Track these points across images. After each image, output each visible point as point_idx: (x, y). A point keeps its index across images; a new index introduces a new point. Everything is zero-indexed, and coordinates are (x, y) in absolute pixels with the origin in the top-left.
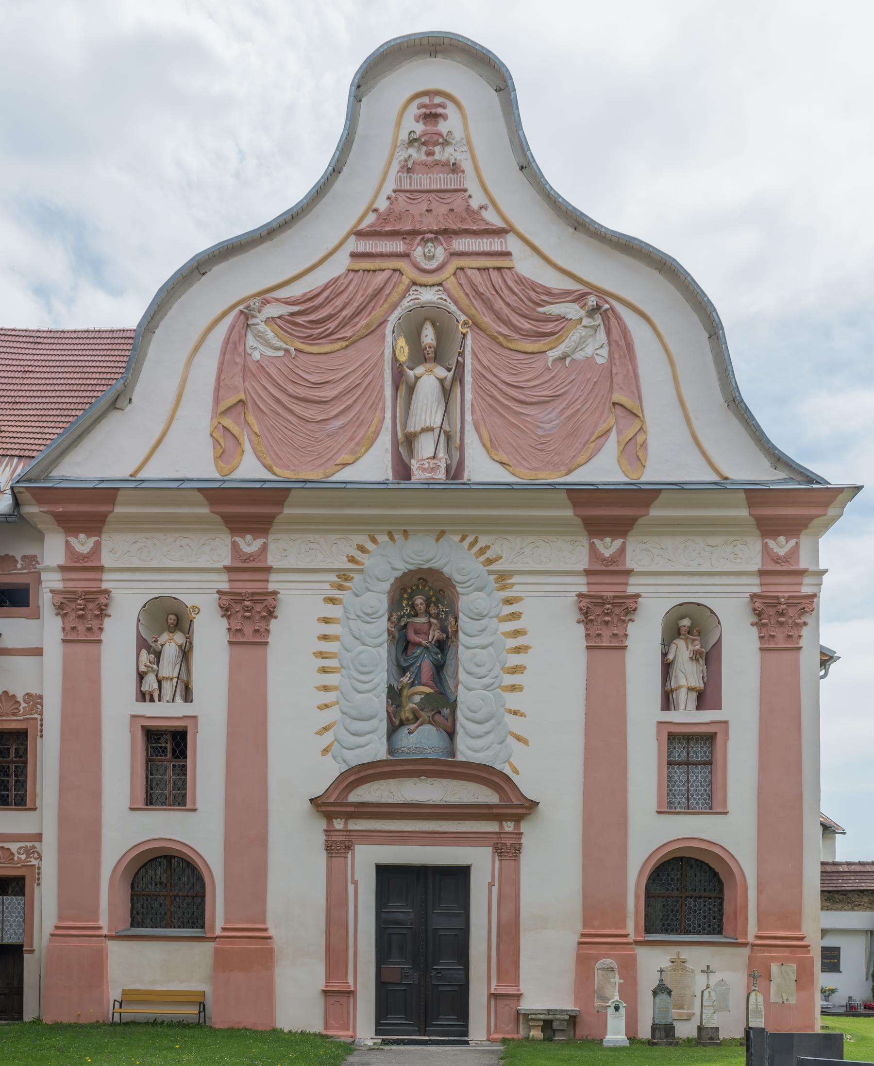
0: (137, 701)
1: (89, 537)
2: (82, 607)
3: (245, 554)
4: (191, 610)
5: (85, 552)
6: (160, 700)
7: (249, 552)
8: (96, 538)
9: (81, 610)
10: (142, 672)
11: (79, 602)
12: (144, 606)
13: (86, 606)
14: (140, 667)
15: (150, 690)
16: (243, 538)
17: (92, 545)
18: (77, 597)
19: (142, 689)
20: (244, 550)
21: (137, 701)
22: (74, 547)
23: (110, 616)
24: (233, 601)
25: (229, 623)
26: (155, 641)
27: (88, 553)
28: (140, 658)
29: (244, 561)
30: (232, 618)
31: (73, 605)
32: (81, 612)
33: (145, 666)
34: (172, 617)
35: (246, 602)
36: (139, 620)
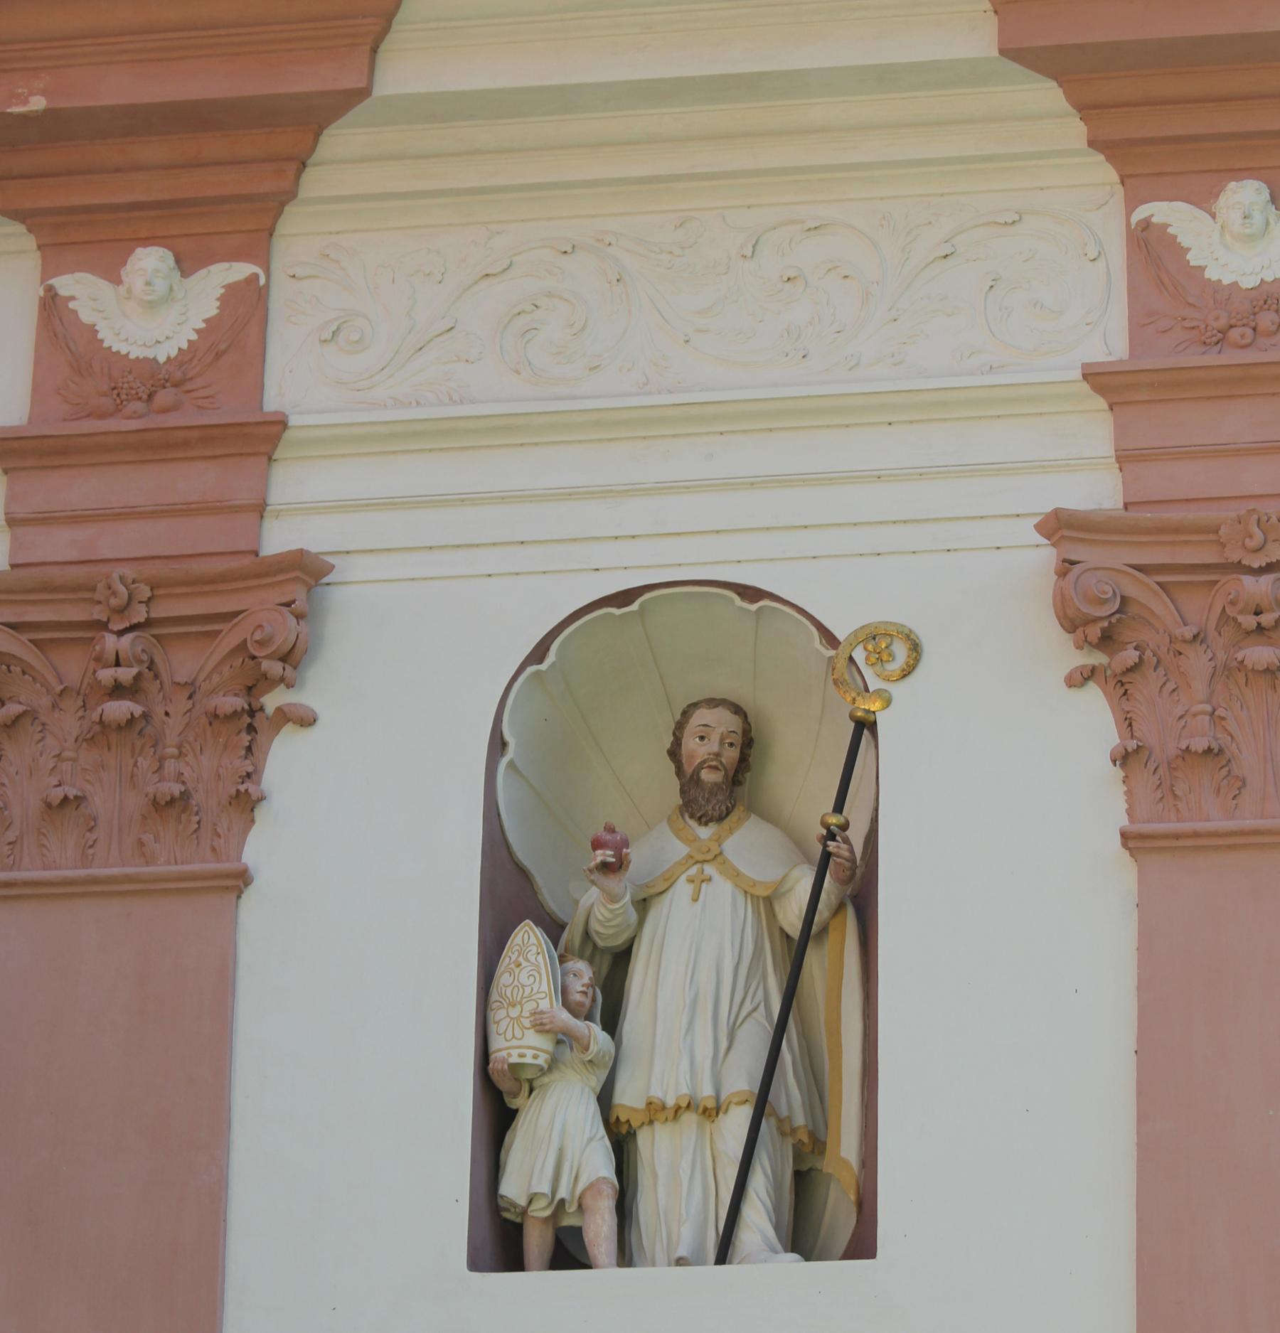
0: (475, 1264)
1: (187, 264)
2: (126, 674)
3: (1225, 294)
4: (859, 655)
5: (163, 353)
6: (625, 1256)
7: (1248, 283)
8: (241, 270)
9: (118, 690)
10: (515, 1067)
11: (111, 643)
12: (539, 653)
13: (151, 666)
14: (496, 1043)
15: (563, 1193)
16: (1205, 200)
17: (212, 310)
18: (98, 614)
19: (512, 1188)
20: (1211, 274)
21: (475, 1264)
22: (92, 330)
23: (307, 720)
24: (1151, 581)
25: (1127, 723)
26: (605, 867)
27: (185, 358)
28: (503, 979)
29: (1221, 339)
30: (1146, 687)
31: (73, 666)
32: (119, 709)
33: (540, 1027)
34: (722, 721)
35: (1248, 580)
36: (498, 744)
